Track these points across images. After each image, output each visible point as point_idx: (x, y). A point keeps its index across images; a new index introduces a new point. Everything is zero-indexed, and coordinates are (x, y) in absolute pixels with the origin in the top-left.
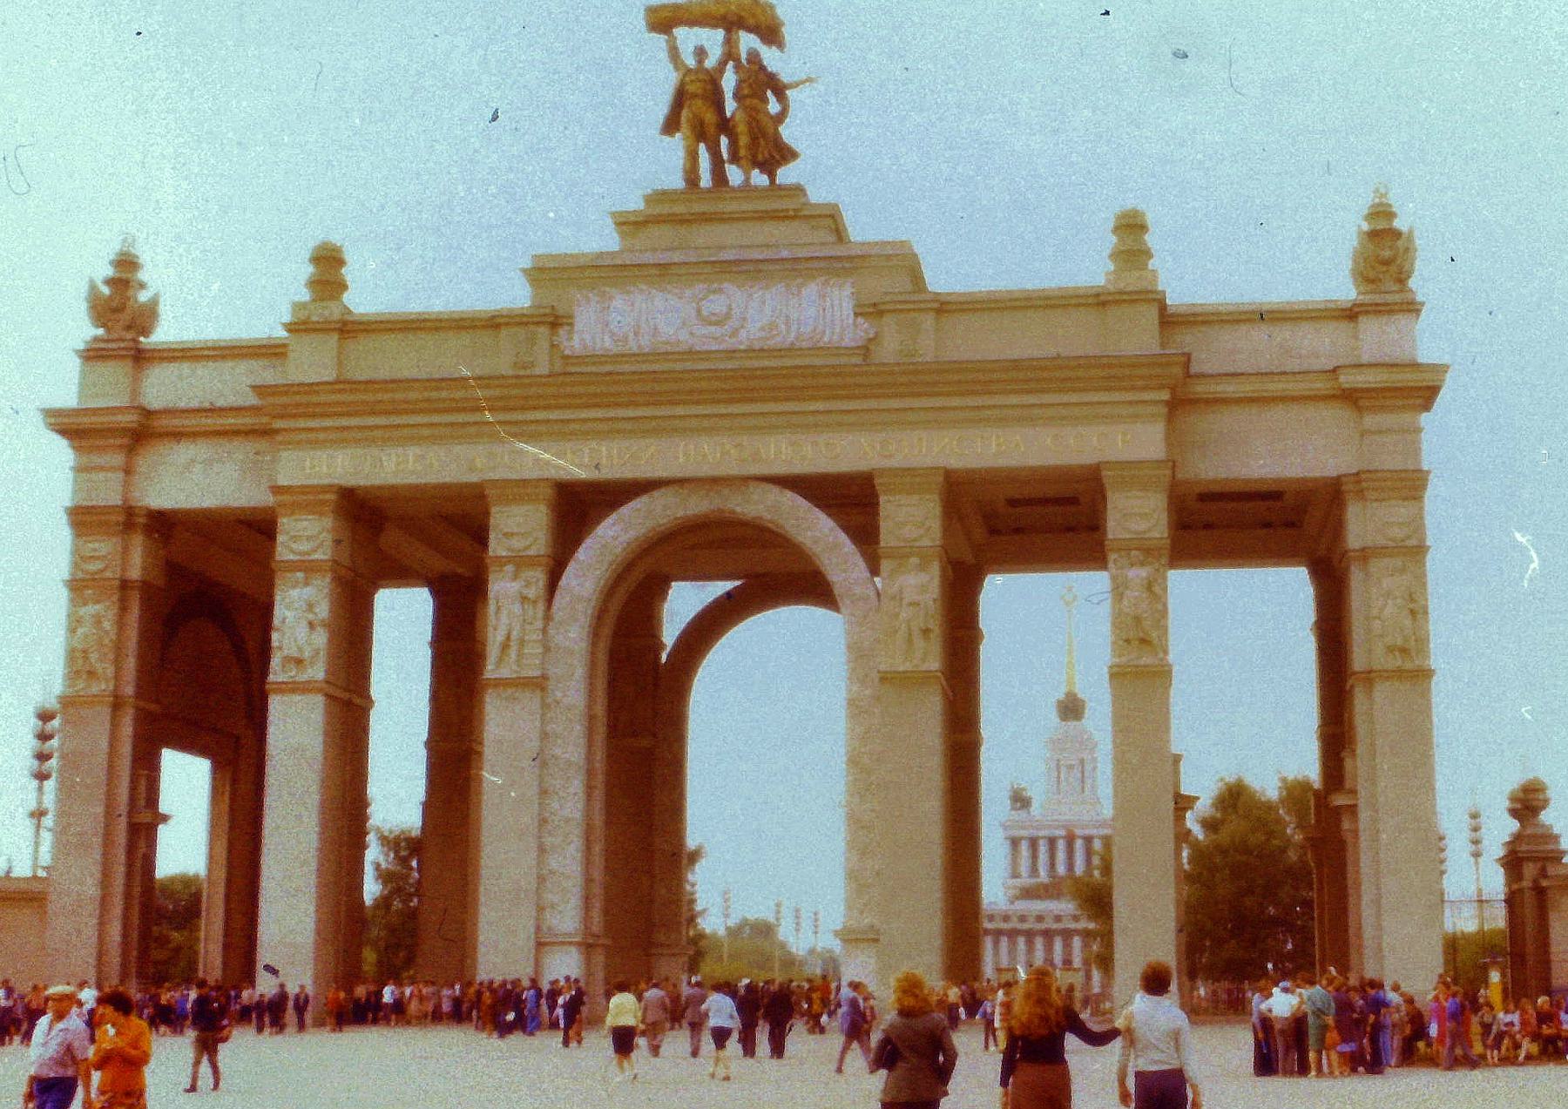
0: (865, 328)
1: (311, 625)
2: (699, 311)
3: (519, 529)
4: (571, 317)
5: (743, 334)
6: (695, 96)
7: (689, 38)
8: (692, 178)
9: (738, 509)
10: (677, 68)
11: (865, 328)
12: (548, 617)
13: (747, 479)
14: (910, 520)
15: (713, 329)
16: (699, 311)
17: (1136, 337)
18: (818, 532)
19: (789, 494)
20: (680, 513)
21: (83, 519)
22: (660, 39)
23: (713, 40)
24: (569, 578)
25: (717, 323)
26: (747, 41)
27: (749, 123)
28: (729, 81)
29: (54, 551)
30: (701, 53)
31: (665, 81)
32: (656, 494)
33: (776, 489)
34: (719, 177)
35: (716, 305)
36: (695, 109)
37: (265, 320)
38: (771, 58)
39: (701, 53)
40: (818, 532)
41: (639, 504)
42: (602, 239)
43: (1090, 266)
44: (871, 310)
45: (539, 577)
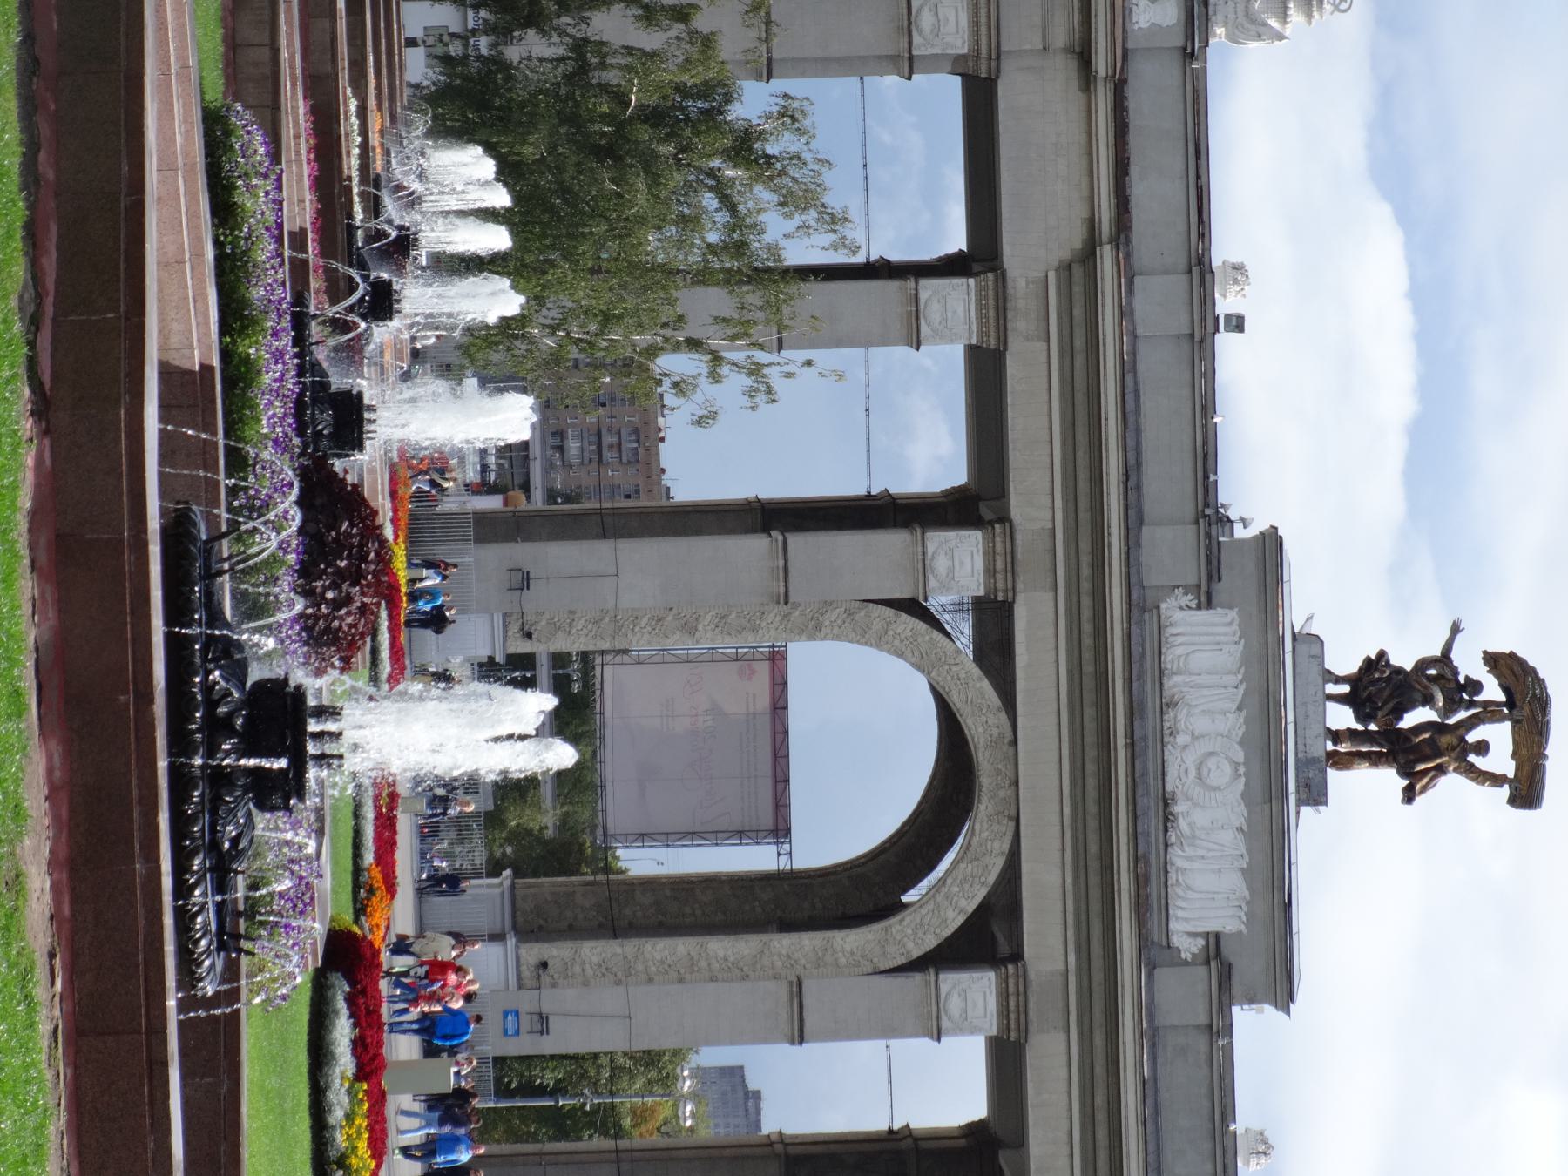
2: (1211, 754)
4: (1210, 605)
15: (1193, 773)
16: (1211, 754)
25: (1199, 776)
32: (1003, 716)
35: (1220, 772)
41: (993, 698)
44: (1214, 948)
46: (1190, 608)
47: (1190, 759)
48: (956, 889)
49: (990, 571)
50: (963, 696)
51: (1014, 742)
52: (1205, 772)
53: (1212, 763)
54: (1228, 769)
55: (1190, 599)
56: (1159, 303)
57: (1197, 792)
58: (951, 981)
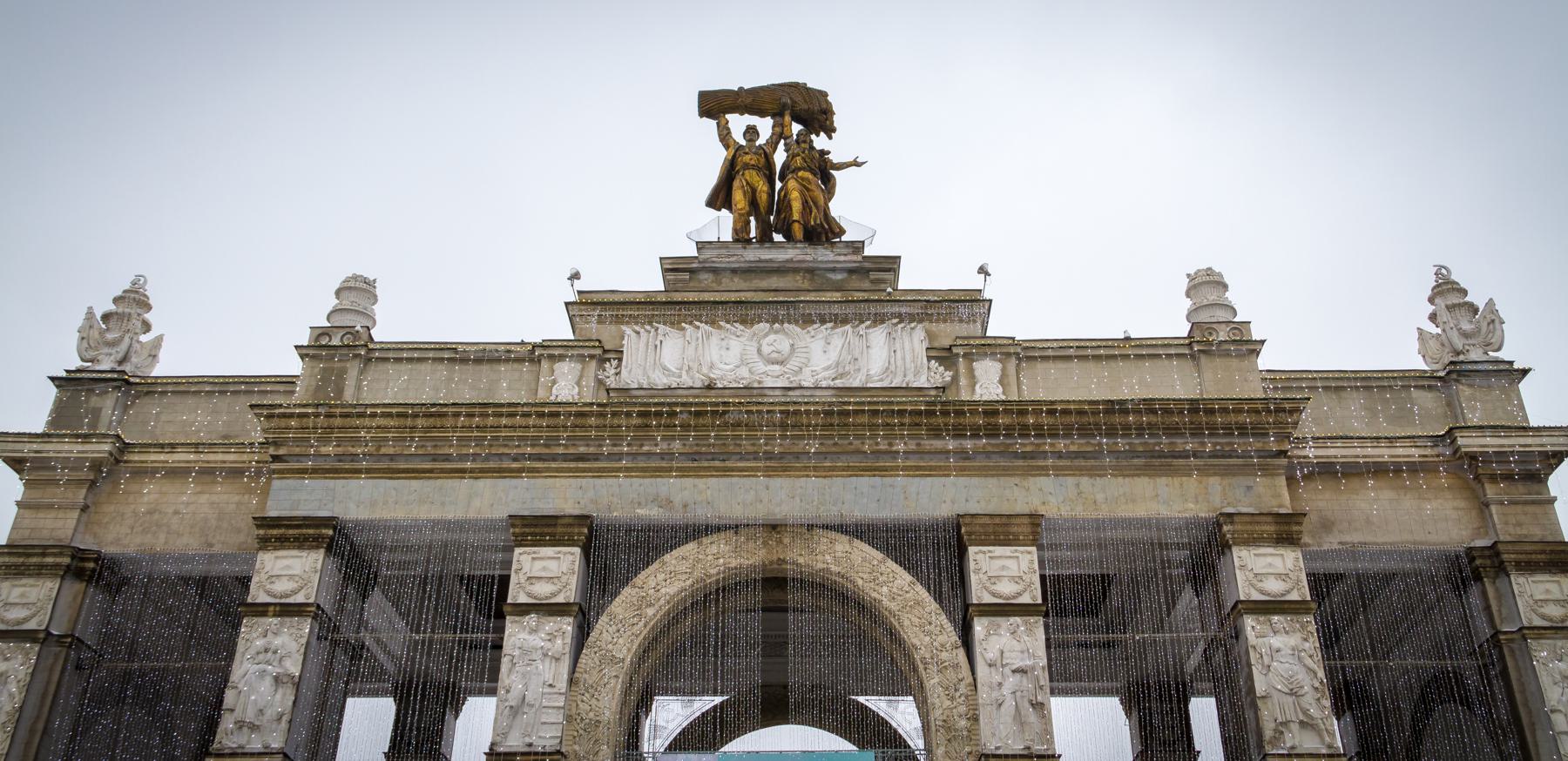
0: (941, 375)
1: (277, 680)
2: (759, 351)
3: (547, 571)
5: (807, 371)
6: (746, 166)
7: (738, 123)
9: (801, 560)
10: (727, 147)
11: (941, 375)
12: (572, 681)
13: (811, 527)
14: (1003, 571)
15: (777, 367)
16: (759, 351)
18: (894, 588)
19: (857, 542)
20: (734, 563)
22: (711, 124)
23: (765, 126)
24: (603, 629)
25: (781, 363)
26: (796, 128)
27: (801, 193)
28: (780, 157)
30: (751, 132)
31: (718, 157)
32: (705, 540)
33: (845, 538)
37: (277, 355)
38: (820, 142)
39: (751, 132)
40: (894, 588)
42: (654, 282)
43: (1170, 320)
44: (944, 356)
45: (567, 625)
46: (619, 365)
47: (761, 367)
48: (885, 589)
49: (556, 542)
50: (684, 577)
51: (736, 528)
52: (775, 355)
53: (766, 350)
54: (772, 337)
55: (610, 369)
57: (793, 364)
58: (979, 593)
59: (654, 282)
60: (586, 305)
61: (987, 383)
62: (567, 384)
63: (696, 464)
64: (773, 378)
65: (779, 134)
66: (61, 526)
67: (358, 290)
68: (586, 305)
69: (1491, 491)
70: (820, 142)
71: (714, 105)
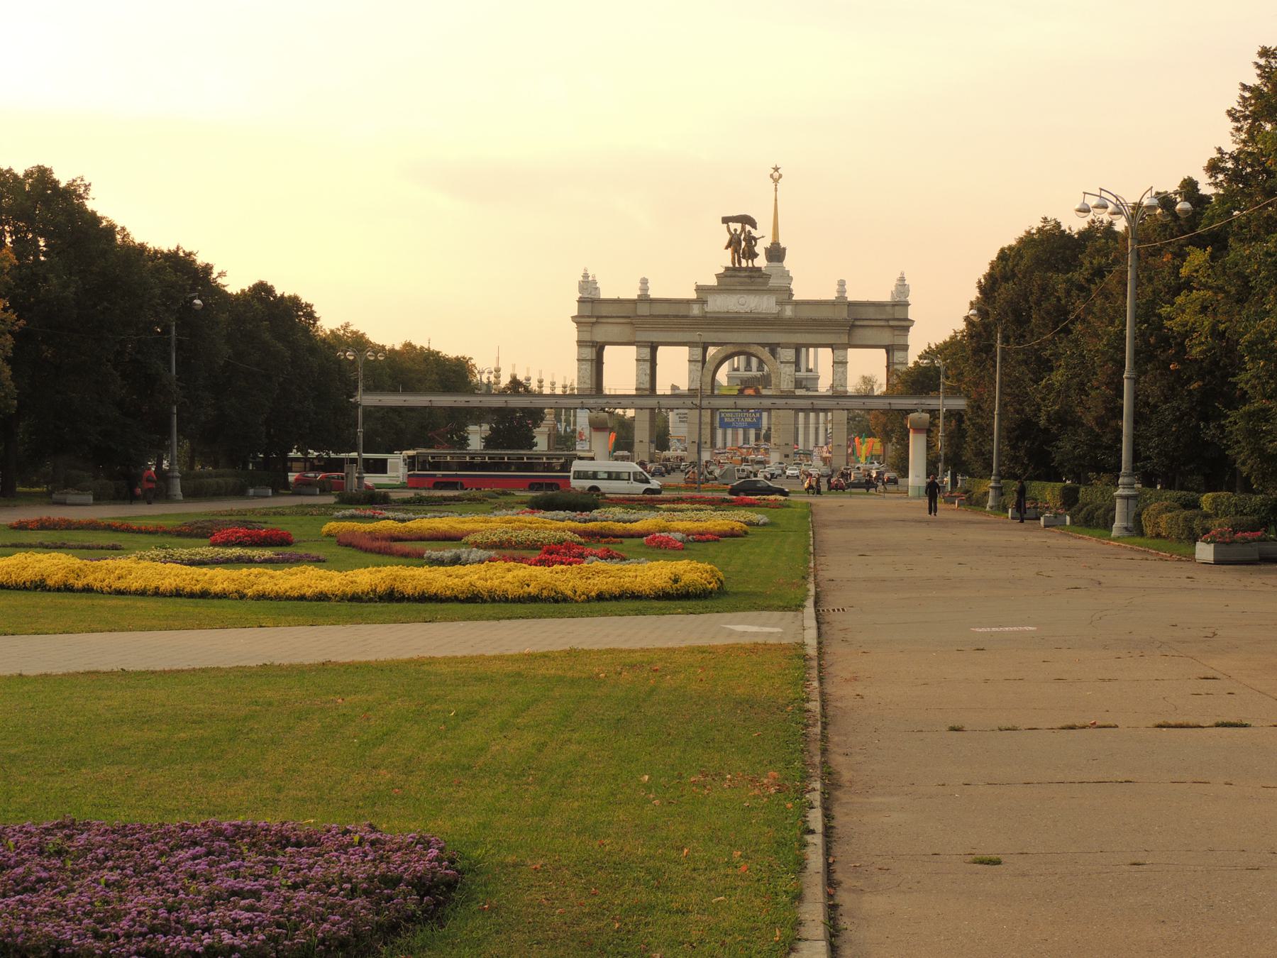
7: (733, 226)
8: (733, 263)
11: (778, 308)
17: (843, 314)
21: (581, 343)
23: (738, 226)
26: (748, 228)
29: (573, 350)
31: (728, 237)
34: (740, 262)
35: (742, 300)
36: (734, 243)
38: (754, 233)
42: (713, 282)
43: (831, 295)
44: (779, 303)
45: (700, 364)
56: (643, 310)
59: (713, 282)
60: (699, 289)
61: (789, 312)
62: (696, 310)
63: (726, 330)
64: (742, 309)
65: (743, 229)
66: (587, 337)
67: (644, 282)
68: (699, 289)
69: (897, 332)
70: (753, 231)
71: (726, 220)
